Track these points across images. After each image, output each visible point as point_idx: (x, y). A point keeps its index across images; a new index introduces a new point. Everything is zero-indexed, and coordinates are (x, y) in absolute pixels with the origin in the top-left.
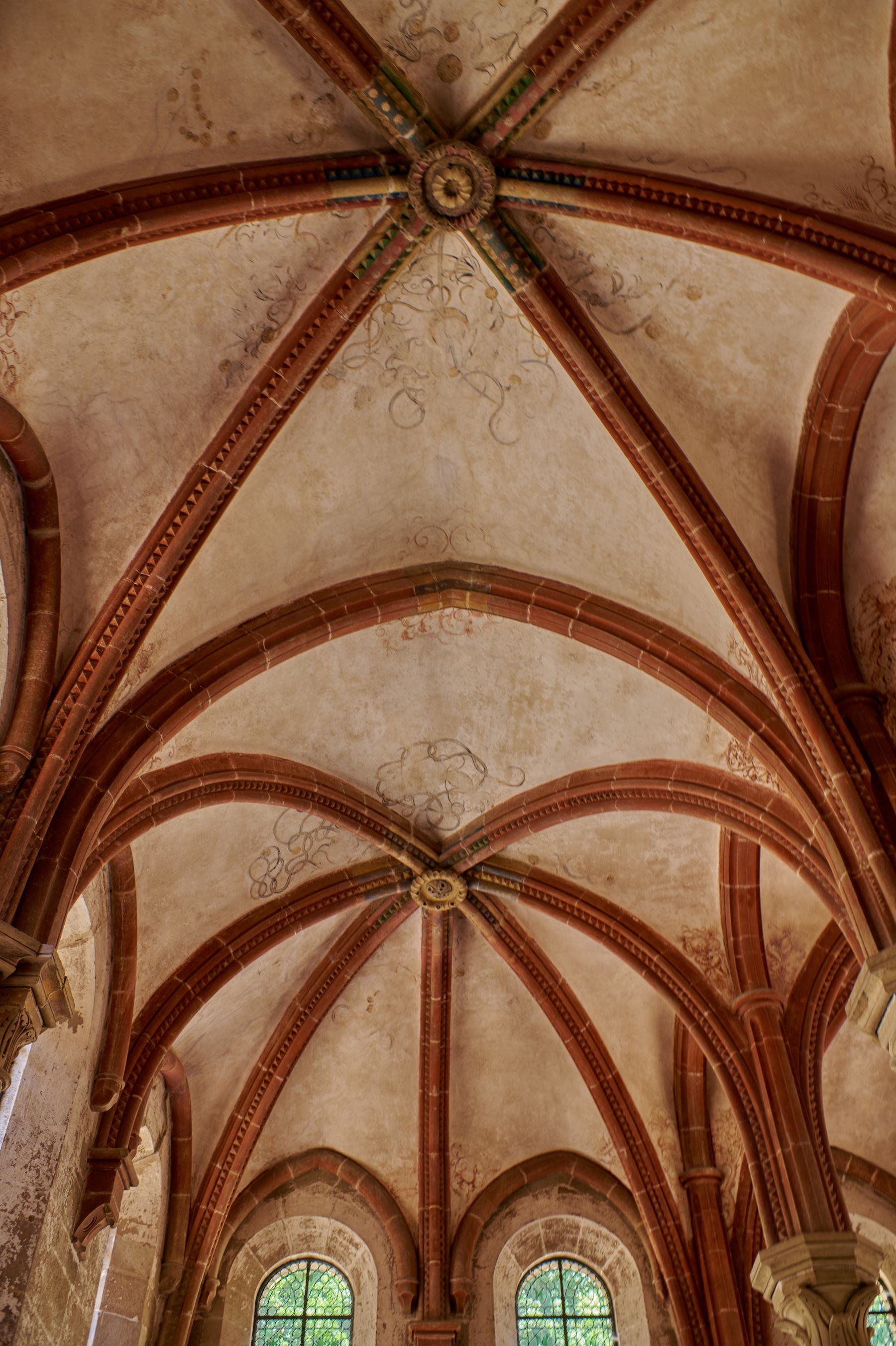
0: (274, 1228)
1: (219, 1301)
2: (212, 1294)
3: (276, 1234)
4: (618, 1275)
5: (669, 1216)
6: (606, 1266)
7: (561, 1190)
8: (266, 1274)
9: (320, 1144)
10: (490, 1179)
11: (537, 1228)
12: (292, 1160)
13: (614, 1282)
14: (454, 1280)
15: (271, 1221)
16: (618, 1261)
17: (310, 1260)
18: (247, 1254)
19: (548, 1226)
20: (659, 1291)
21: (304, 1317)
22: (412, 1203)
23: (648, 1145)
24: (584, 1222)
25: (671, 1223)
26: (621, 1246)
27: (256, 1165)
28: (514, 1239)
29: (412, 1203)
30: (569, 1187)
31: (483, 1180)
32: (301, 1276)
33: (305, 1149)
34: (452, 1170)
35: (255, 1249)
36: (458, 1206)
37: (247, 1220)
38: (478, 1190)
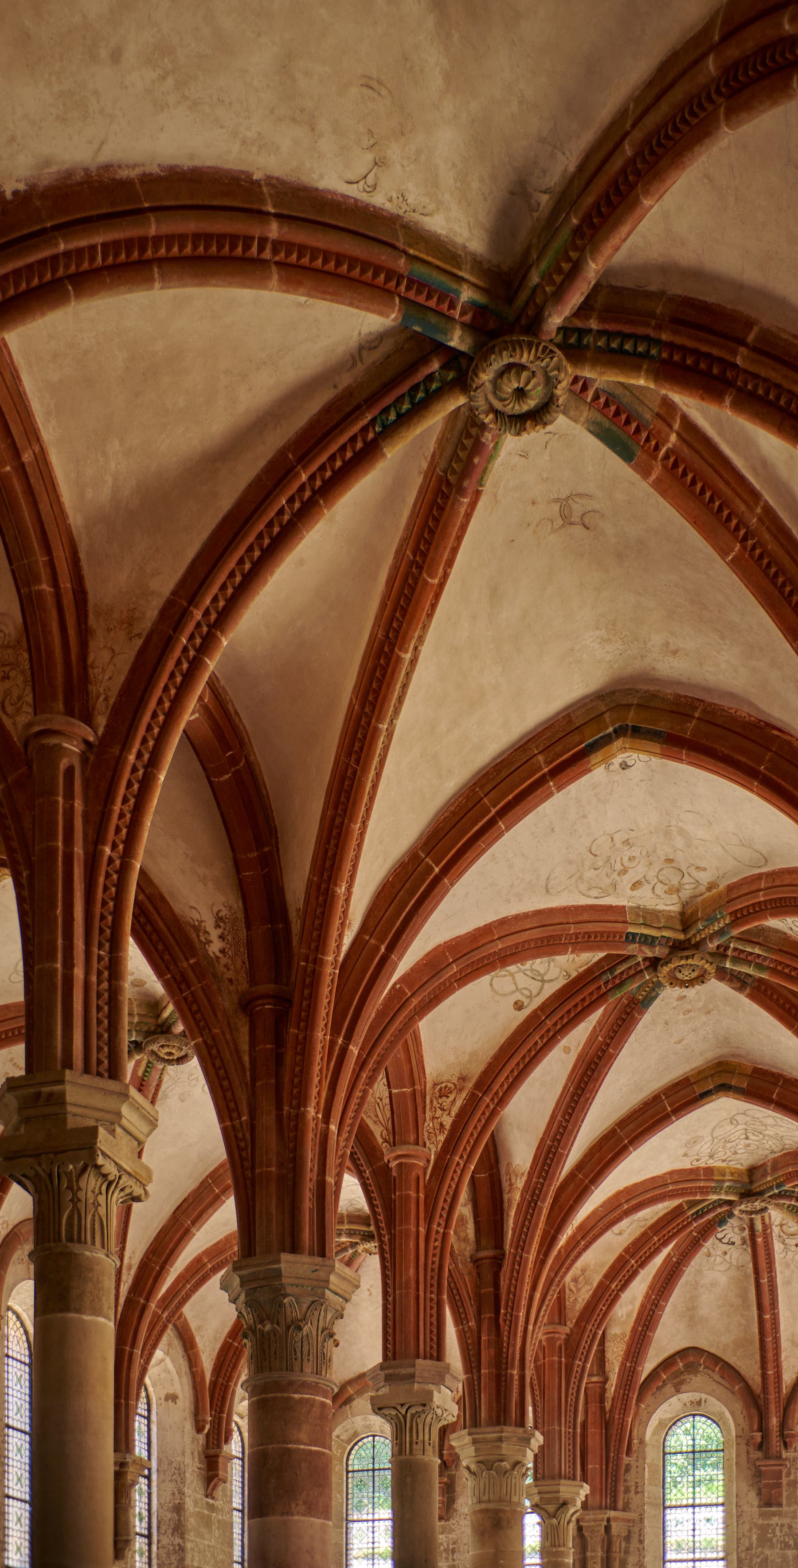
0: (347, 1424)
3: (349, 1426)
8: (349, 1447)
12: (350, 1382)
15: (344, 1420)
17: (374, 1436)
21: (374, 1470)
32: (370, 1445)
33: (357, 1374)
35: (338, 1437)
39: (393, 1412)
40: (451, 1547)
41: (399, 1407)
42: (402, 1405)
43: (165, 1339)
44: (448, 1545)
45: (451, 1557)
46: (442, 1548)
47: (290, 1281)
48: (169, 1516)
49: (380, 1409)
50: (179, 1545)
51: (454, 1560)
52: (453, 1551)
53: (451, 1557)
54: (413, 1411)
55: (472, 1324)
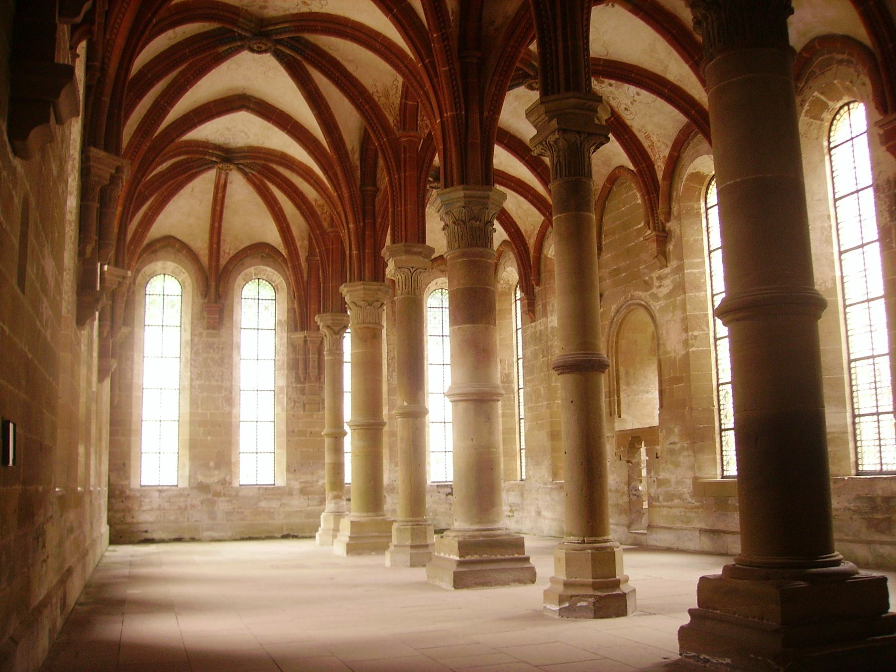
1: (134, 292)
4: (279, 287)
5: (299, 273)
6: (275, 284)
7: (262, 257)
9: (169, 234)
10: (235, 252)
11: (252, 270)
13: (278, 289)
14: (220, 289)
16: (280, 283)
19: (256, 269)
20: (293, 297)
23: (296, 249)
24: (269, 269)
25: (300, 276)
26: (281, 278)
27: (146, 242)
28: (243, 274)
29: (205, 260)
30: (265, 255)
31: (233, 253)
34: (221, 249)
36: (223, 262)
37: (141, 262)
38: (231, 255)
39: (407, 270)
40: (221, 346)
41: (411, 269)
42: (413, 268)
44: (219, 344)
45: (221, 352)
47: (492, 201)
49: (399, 268)
51: (222, 354)
52: (222, 349)
53: (221, 352)
54: (418, 271)
55: (362, 224)
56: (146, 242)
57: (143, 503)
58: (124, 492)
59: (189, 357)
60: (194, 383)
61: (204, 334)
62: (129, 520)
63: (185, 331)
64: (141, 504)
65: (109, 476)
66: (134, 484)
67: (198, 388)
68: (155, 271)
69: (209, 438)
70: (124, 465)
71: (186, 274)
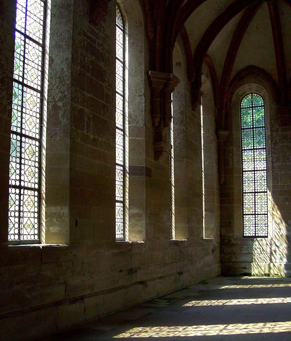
2: (228, 106)
12: (243, 70)
18: (235, 95)
22: (276, 77)
27: (233, 73)
29: (276, 77)
43: (177, 39)
46: (288, 138)
48: (178, 116)
50: (183, 129)
56: (233, 73)
57: (243, 249)
58: (230, 241)
59: (270, 147)
60: (274, 165)
61: (280, 130)
62: (234, 260)
63: (267, 129)
64: (241, 249)
65: (220, 230)
66: (236, 234)
67: (278, 168)
68: (244, 93)
69: (287, 203)
70: (230, 223)
71: (265, 90)
